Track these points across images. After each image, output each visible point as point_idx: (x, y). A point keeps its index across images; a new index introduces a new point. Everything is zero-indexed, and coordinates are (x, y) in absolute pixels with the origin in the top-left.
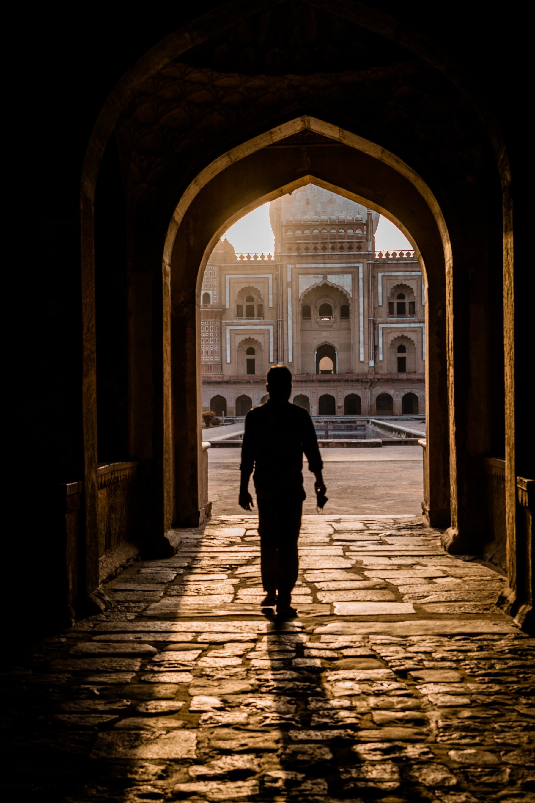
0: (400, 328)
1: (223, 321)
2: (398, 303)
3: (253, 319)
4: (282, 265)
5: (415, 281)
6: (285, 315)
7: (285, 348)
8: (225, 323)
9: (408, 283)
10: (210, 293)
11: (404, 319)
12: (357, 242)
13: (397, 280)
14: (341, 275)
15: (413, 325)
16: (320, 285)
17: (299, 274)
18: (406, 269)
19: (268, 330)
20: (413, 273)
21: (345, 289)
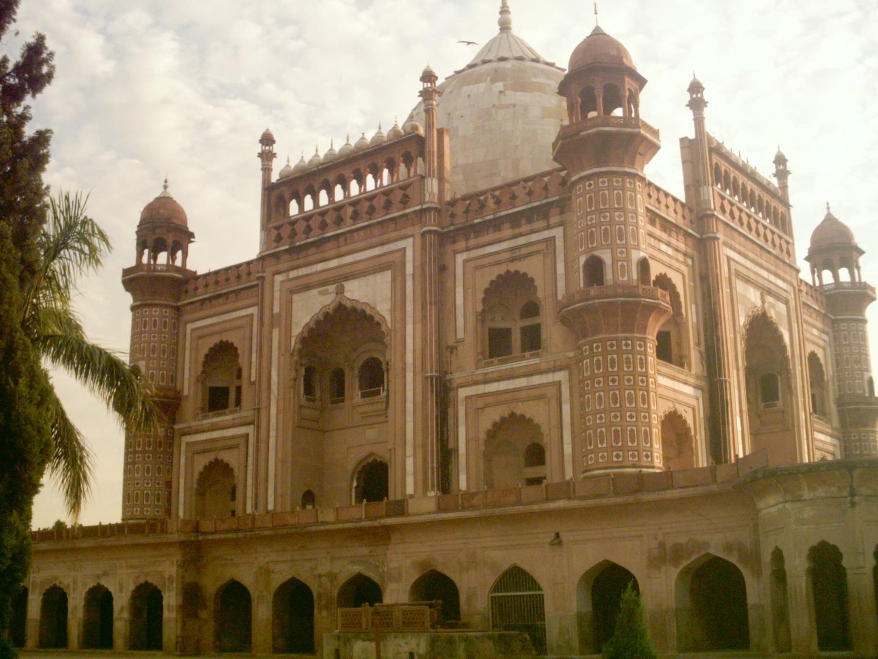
0: (506, 392)
1: (176, 427)
2: (524, 330)
3: (224, 414)
4: (263, 278)
5: (540, 257)
6: (264, 395)
7: (262, 475)
8: (180, 429)
9: (521, 267)
10: (142, 364)
11: (514, 365)
12: (401, 188)
13: (498, 263)
14: (371, 278)
15: (536, 380)
16: (332, 307)
17: (293, 291)
18: (517, 231)
19: (247, 436)
20: (534, 237)
21: (379, 308)
